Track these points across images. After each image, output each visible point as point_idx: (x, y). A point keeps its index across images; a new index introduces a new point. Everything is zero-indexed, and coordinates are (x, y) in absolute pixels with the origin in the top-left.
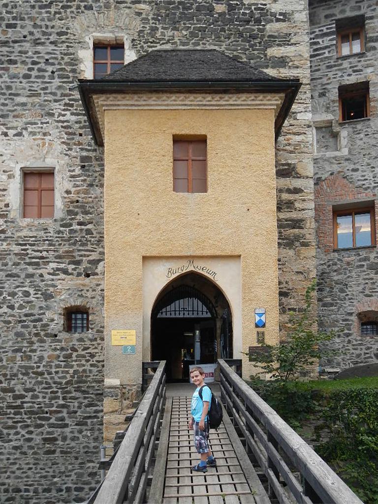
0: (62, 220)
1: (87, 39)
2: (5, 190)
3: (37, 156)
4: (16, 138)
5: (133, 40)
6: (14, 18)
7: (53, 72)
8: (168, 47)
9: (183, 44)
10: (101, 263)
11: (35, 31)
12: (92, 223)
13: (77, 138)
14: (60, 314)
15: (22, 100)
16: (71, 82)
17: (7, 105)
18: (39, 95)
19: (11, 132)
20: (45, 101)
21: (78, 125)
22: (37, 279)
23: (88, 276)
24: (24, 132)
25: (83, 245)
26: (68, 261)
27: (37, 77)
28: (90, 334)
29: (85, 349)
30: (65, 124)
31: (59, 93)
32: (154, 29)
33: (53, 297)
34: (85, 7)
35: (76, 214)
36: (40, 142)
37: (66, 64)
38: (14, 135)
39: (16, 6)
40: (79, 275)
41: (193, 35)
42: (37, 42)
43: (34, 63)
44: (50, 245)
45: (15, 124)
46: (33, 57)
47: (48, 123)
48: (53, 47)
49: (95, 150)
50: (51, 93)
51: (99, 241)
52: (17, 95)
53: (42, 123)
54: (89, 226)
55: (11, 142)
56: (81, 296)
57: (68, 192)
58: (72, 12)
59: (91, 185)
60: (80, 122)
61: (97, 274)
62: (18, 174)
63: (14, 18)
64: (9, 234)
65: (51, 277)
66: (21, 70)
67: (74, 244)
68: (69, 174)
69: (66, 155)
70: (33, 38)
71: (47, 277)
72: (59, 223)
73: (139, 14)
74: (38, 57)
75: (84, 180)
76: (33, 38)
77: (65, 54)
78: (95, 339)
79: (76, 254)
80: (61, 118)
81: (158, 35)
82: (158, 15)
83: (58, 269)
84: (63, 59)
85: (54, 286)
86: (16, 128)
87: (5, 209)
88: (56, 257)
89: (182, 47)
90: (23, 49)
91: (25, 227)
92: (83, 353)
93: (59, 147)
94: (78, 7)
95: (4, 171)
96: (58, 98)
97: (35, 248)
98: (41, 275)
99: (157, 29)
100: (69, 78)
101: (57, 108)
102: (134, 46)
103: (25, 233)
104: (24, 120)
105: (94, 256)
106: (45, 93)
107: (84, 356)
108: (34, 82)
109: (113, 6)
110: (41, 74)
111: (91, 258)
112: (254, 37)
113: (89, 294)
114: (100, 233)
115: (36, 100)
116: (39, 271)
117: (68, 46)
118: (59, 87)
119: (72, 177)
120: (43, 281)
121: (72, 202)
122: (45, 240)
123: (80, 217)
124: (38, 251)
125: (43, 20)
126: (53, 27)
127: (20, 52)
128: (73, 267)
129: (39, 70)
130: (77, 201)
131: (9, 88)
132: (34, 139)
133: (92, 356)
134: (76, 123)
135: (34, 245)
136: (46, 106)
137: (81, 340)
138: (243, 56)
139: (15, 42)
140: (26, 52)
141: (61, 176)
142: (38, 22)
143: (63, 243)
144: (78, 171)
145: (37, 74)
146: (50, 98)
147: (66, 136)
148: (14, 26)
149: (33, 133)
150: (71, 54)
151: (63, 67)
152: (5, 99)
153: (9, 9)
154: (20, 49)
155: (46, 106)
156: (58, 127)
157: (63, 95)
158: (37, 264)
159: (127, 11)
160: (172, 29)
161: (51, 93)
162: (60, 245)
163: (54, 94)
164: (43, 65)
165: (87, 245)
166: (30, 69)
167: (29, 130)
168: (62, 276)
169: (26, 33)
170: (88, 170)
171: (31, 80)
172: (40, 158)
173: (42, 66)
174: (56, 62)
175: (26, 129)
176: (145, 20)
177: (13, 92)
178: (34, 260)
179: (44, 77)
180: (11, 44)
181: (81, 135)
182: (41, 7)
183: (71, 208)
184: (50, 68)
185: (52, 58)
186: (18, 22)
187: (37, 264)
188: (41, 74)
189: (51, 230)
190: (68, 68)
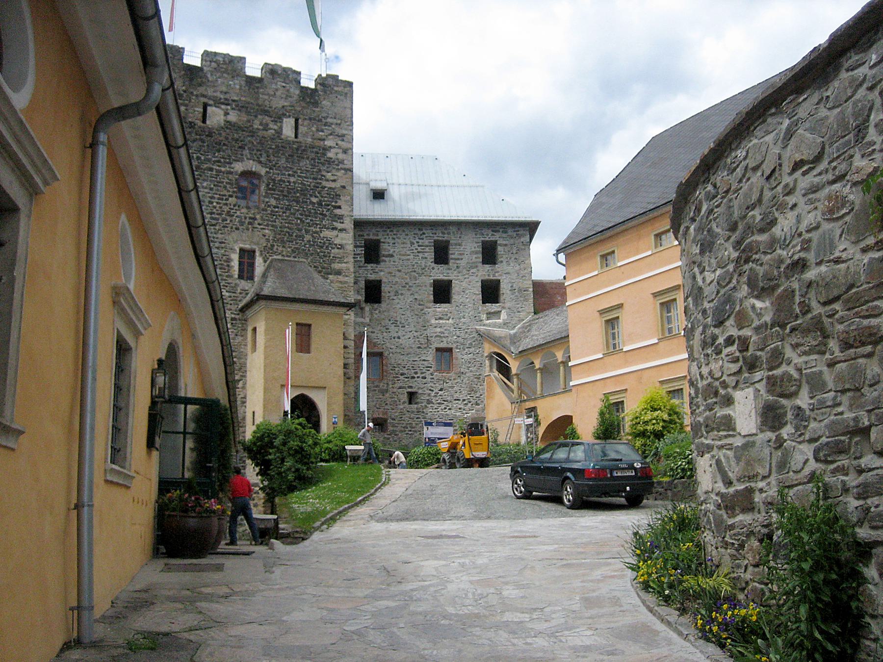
8: (280, 257)
89: (286, 258)
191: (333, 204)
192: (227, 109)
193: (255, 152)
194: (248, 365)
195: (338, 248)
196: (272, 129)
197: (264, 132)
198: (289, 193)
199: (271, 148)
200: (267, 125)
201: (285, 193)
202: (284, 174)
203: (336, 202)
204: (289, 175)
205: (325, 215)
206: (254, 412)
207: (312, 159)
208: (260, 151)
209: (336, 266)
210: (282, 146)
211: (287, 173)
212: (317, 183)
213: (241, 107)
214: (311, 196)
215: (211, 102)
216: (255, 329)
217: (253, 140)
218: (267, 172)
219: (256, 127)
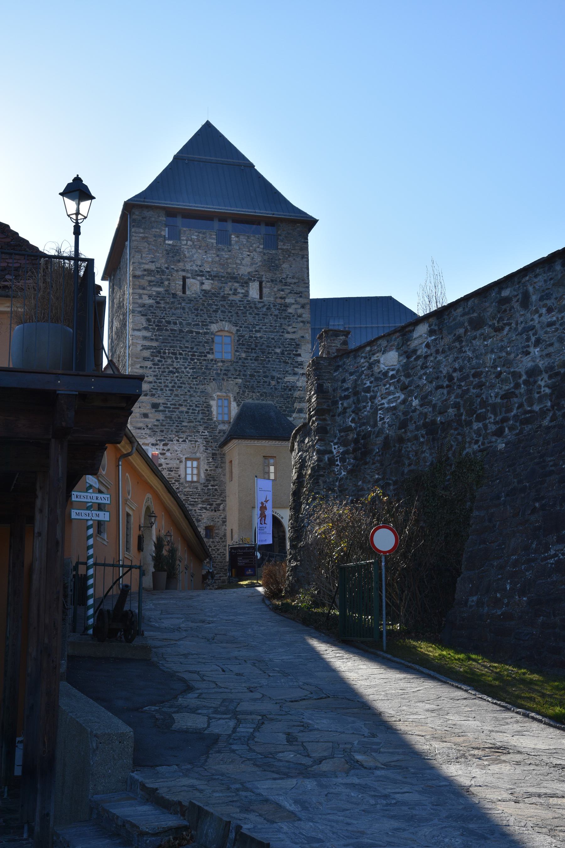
0: (204, 484)
1: (214, 395)
2: (178, 468)
3: (193, 452)
4: (183, 443)
5: (235, 397)
6: (181, 383)
7: (199, 411)
9: (257, 400)
10: (222, 505)
11: (191, 390)
12: (217, 485)
13: (210, 444)
14: (204, 529)
15: (184, 424)
16: (207, 416)
17: (178, 426)
18: (192, 422)
19: (181, 440)
20: (196, 425)
21: (211, 438)
22: (194, 513)
23: (215, 511)
24: (187, 441)
25: (214, 496)
26: (207, 503)
27: (192, 413)
28: (217, 539)
29: (215, 546)
30: (205, 437)
31: (202, 421)
32: (244, 392)
33: (200, 521)
34: (213, 379)
35: (210, 481)
36: (194, 445)
37: (205, 407)
38: (182, 441)
39: (181, 378)
40: (212, 510)
41: (261, 395)
42: (191, 396)
43: (190, 406)
44: (199, 496)
45: (182, 436)
46: (189, 403)
47: (197, 436)
48: (198, 398)
49: (218, 450)
50: (198, 421)
51: (221, 494)
52: (183, 421)
53: (194, 436)
54: (216, 487)
55: (181, 445)
56: (213, 521)
57: (207, 470)
58: (207, 382)
59: (217, 467)
60: (211, 436)
61: (220, 510)
62: (184, 460)
63: (181, 383)
64: (180, 490)
65: (199, 511)
66: (184, 409)
67: (210, 495)
68: (207, 461)
69: (205, 452)
70: (190, 393)
71: (198, 511)
72: (203, 485)
73: (236, 384)
74: (192, 403)
75: (214, 465)
76: (190, 393)
77: (205, 402)
78: (219, 542)
79: (210, 500)
80: (203, 434)
81: (246, 395)
82: (246, 385)
83: (203, 508)
84: (203, 405)
85: (201, 516)
86: (182, 438)
87: (178, 477)
88: (202, 502)
90: (185, 399)
91: (187, 487)
92: (214, 548)
93: (202, 448)
94: (210, 379)
95: (178, 459)
96: (201, 424)
97: (192, 497)
98: (195, 510)
99: (245, 391)
100: (206, 414)
101: (201, 429)
102: (235, 400)
103: (187, 490)
104: (186, 434)
105: (219, 502)
106: (196, 421)
107: (214, 550)
108: (190, 415)
109: (226, 380)
110: (194, 411)
111: (217, 503)
112: (288, 398)
113: (217, 520)
114: (221, 490)
115: (192, 424)
116: (194, 508)
117: (205, 399)
118: (202, 419)
119: (208, 462)
120: (196, 513)
121: (208, 475)
122: (196, 493)
123: (212, 483)
124: (193, 498)
125: (194, 385)
126: (199, 389)
127: (184, 400)
128: (209, 506)
129: (193, 410)
130: (210, 475)
131: (179, 418)
132: (191, 444)
133: (218, 550)
134: (210, 436)
135: (192, 495)
136: (196, 427)
137: (213, 542)
138: (284, 407)
139: (181, 395)
140: (187, 401)
141: (203, 462)
142: (192, 386)
143: (205, 495)
144: (211, 460)
145: (192, 411)
146: (198, 424)
147: (205, 443)
148: (181, 387)
149: (190, 441)
150: (207, 402)
151: (203, 408)
152: (178, 424)
153: (179, 378)
154: (184, 399)
155: (196, 427)
156: (201, 438)
157: (203, 422)
158: (193, 505)
159: (232, 382)
160: (253, 392)
161: (198, 421)
162: (203, 496)
163: (200, 422)
164: (194, 407)
165: (215, 496)
166: (189, 409)
167: (189, 439)
168: (204, 511)
169: (186, 391)
170: (215, 460)
171: (190, 414)
172: (194, 453)
173: (194, 407)
174: (200, 406)
175: (187, 438)
176: (240, 387)
177: (181, 420)
178: (192, 503)
179: (194, 413)
180: (180, 396)
181: (212, 442)
182: (193, 378)
183: (208, 478)
184: (197, 409)
185: (198, 404)
186: (183, 385)
187: (193, 505)
188: (194, 411)
189: (199, 488)
190: (206, 409)
191: (294, 352)
192: (203, 280)
193: (227, 313)
194: (227, 491)
195: (299, 390)
196: (239, 293)
197: (234, 297)
198: (256, 346)
199: (240, 310)
200: (236, 290)
201: (253, 346)
202: (252, 331)
203: (297, 351)
204: (256, 331)
205: (288, 363)
206: (232, 530)
207: (275, 315)
208: (231, 312)
209: (297, 405)
210: (250, 306)
211: (254, 330)
212: (280, 336)
213: (213, 277)
214: (275, 347)
215: (189, 275)
216: (231, 462)
217: (224, 303)
218: (238, 330)
219: (226, 292)
